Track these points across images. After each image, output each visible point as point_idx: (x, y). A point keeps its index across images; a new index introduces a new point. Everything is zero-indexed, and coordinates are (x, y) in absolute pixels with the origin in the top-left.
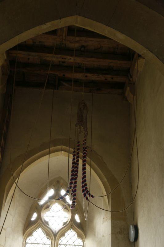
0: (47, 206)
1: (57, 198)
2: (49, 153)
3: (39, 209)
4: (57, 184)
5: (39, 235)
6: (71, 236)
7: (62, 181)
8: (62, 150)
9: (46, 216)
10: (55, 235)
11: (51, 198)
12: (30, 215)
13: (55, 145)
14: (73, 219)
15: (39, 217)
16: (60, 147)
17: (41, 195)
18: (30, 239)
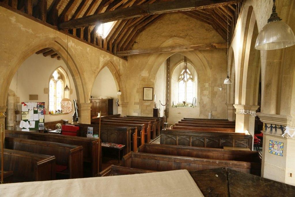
6: (190, 81)
12: (179, 77)
14: (190, 77)
17: (181, 71)
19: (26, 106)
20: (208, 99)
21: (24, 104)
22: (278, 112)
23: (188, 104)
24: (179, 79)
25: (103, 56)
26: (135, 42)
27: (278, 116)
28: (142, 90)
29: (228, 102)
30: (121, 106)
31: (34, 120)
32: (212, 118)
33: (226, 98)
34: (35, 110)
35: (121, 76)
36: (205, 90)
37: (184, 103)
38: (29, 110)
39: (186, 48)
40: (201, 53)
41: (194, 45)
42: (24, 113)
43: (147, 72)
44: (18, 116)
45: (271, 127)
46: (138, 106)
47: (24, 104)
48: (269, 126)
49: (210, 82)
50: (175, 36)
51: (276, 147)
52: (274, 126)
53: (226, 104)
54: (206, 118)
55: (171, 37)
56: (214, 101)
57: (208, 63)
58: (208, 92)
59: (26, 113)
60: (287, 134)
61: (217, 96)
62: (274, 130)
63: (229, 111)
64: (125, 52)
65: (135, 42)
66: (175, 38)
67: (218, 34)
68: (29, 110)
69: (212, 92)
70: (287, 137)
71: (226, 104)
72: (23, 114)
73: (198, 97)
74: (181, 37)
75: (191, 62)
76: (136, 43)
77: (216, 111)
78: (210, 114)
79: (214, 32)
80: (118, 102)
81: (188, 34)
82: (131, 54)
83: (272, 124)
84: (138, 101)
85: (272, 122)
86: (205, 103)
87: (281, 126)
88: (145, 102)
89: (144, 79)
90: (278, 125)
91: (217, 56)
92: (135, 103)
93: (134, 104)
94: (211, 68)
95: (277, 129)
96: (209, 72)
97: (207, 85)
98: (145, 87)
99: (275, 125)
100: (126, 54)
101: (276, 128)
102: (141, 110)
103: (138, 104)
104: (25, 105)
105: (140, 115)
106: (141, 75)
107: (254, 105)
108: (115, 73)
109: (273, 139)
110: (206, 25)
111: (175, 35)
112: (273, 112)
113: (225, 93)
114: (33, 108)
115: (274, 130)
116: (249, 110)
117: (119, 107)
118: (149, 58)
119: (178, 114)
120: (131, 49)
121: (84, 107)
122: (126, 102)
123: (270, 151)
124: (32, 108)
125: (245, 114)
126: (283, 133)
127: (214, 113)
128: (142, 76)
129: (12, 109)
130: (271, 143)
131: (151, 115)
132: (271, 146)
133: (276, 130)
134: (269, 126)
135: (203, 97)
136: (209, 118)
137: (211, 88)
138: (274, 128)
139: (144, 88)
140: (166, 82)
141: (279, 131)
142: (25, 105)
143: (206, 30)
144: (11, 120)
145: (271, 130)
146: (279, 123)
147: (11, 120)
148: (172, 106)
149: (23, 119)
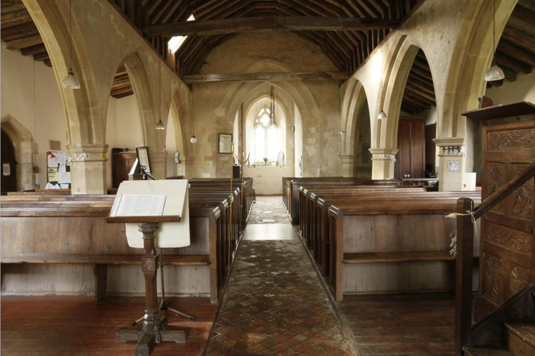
0: (261, 117)
1: (265, 112)
2: (261, 98)
3: (259, 118)
4: (265, 107)
5: (259, 127)
7: (267, 106)
8: (266, 96)
9: (261, 120)
10: (266, 128)
11: (263, 114)
12: (255, 121)
13: (263, 95)
15: (259, 122)
16: (265, 96)
17: (258, 113)
18: (257, 130)
19: (54, 159)
20: (315, 150)
21: (50, 156)
22: (454, 134)
23: (270, 163)
24: (255, 124)
25: (173, 81)
26: (205, 63)
27: (455, 138)
28: (216, 138)
29: (342, 154)
30: (184, 163)
31: (67, 183)
32: (322, 176)
33: (340, 148)
34: (67, 165)
35: (186, 114)
36: (310, 137)
37: (266, 160)
38: (59, 164)
39: (292, 76)
40: (306, 84)
41: (303, 72)
42: (52, 170)
43: (224, 109)
44: (37, 175)
45: (449, 149)
46: (211, 163)
47: (50, 156)
48: (446, 148)
49: (318, 126)
50: (267, 57)
51: (453, 165)
52: (451, 147)
53: (340, 156)
54: (312, 176)
55: (262, 58)
56: (323, 152)
57: (315, 99)
58: (315, 139)
59: (55, 170)
60: (462, 152)
61: (327, 145)
62: (451, 151)
63: (344, 165)
64: (191, 77)
65: (205, 63)
66: (268, 60)
67: (328, 59)
68: (59, 164)
69: (320, 139)
70: (463, 155)
71: (340, 156)
72: (49, 173)
73: (287, 150)
74: (277, 60)
75: (278, 97)
76: (206, 64)
77: (327, 165)
78: (318, 170)
79: (322, 56)
80: (179, 156)
81: (286, 56)
82: (208, 81)
83: (449, 146)
84: (210, 154)
85: (450, 144)
86: (309, 156)
87: (458, 146)
88: (221, 156)
89: (219, 121)
90: (455, 146)
91: (327, 90)
92: (206, 158)
93: (205, 160)
94: (319, 106)
95: (454, 150)
96: (317, 112)
97: (313, 130)
98: (221, 132)
99: (453, 146)
100: (200, 81)
101: (453, 149)
102: (217, 168)
103: (210, 159)
104: (53, 156)
105: (214, 177)
106: (214, 114)
107: (394, 148)
108: (180, 109)
109: (450, 158)
110: (312, 45)
111: (268, 56)
112: (450, 136)
113: (338, 141)
114: (65, 161)
115: (451, 151)
116: (390, 154)
117: (180, 165)
118: (227, 89)
119: (258, 178)
120: (198, 73)
121: (158, 157)
122: (191, 156)
123: (448, 169)
124: (63, 161)
125: (385, 159)
126: (459, 151)
127: (324, 169)
128: (216, 115)
129: (29, 164)
130: (448, 162)
131: (229, 176)
132: (449, 166)
133: (453, 151)
134: (446, 148)
135: (307, 148)
136: (318, 176)
137: (319, 134)
138: (451, 149)
139: (219, 134)
140: (239, 129)
141: (456, 151)
142: (53, 156)
143: (313, 52)
144: (28, 182)
145: (449, 151)
146: (456, 144)
147: (28, 182)
148: (248, 166)
149: (51, 180)
